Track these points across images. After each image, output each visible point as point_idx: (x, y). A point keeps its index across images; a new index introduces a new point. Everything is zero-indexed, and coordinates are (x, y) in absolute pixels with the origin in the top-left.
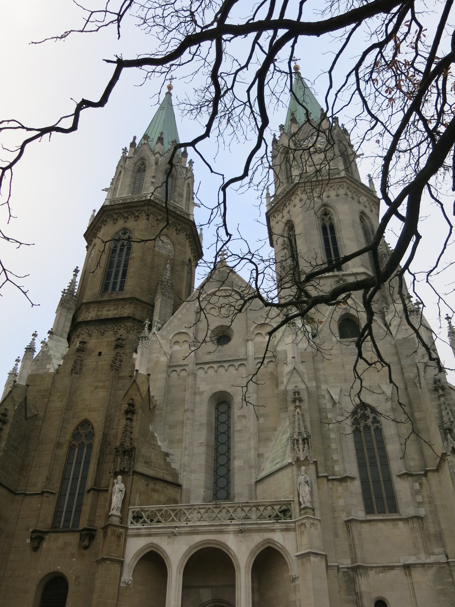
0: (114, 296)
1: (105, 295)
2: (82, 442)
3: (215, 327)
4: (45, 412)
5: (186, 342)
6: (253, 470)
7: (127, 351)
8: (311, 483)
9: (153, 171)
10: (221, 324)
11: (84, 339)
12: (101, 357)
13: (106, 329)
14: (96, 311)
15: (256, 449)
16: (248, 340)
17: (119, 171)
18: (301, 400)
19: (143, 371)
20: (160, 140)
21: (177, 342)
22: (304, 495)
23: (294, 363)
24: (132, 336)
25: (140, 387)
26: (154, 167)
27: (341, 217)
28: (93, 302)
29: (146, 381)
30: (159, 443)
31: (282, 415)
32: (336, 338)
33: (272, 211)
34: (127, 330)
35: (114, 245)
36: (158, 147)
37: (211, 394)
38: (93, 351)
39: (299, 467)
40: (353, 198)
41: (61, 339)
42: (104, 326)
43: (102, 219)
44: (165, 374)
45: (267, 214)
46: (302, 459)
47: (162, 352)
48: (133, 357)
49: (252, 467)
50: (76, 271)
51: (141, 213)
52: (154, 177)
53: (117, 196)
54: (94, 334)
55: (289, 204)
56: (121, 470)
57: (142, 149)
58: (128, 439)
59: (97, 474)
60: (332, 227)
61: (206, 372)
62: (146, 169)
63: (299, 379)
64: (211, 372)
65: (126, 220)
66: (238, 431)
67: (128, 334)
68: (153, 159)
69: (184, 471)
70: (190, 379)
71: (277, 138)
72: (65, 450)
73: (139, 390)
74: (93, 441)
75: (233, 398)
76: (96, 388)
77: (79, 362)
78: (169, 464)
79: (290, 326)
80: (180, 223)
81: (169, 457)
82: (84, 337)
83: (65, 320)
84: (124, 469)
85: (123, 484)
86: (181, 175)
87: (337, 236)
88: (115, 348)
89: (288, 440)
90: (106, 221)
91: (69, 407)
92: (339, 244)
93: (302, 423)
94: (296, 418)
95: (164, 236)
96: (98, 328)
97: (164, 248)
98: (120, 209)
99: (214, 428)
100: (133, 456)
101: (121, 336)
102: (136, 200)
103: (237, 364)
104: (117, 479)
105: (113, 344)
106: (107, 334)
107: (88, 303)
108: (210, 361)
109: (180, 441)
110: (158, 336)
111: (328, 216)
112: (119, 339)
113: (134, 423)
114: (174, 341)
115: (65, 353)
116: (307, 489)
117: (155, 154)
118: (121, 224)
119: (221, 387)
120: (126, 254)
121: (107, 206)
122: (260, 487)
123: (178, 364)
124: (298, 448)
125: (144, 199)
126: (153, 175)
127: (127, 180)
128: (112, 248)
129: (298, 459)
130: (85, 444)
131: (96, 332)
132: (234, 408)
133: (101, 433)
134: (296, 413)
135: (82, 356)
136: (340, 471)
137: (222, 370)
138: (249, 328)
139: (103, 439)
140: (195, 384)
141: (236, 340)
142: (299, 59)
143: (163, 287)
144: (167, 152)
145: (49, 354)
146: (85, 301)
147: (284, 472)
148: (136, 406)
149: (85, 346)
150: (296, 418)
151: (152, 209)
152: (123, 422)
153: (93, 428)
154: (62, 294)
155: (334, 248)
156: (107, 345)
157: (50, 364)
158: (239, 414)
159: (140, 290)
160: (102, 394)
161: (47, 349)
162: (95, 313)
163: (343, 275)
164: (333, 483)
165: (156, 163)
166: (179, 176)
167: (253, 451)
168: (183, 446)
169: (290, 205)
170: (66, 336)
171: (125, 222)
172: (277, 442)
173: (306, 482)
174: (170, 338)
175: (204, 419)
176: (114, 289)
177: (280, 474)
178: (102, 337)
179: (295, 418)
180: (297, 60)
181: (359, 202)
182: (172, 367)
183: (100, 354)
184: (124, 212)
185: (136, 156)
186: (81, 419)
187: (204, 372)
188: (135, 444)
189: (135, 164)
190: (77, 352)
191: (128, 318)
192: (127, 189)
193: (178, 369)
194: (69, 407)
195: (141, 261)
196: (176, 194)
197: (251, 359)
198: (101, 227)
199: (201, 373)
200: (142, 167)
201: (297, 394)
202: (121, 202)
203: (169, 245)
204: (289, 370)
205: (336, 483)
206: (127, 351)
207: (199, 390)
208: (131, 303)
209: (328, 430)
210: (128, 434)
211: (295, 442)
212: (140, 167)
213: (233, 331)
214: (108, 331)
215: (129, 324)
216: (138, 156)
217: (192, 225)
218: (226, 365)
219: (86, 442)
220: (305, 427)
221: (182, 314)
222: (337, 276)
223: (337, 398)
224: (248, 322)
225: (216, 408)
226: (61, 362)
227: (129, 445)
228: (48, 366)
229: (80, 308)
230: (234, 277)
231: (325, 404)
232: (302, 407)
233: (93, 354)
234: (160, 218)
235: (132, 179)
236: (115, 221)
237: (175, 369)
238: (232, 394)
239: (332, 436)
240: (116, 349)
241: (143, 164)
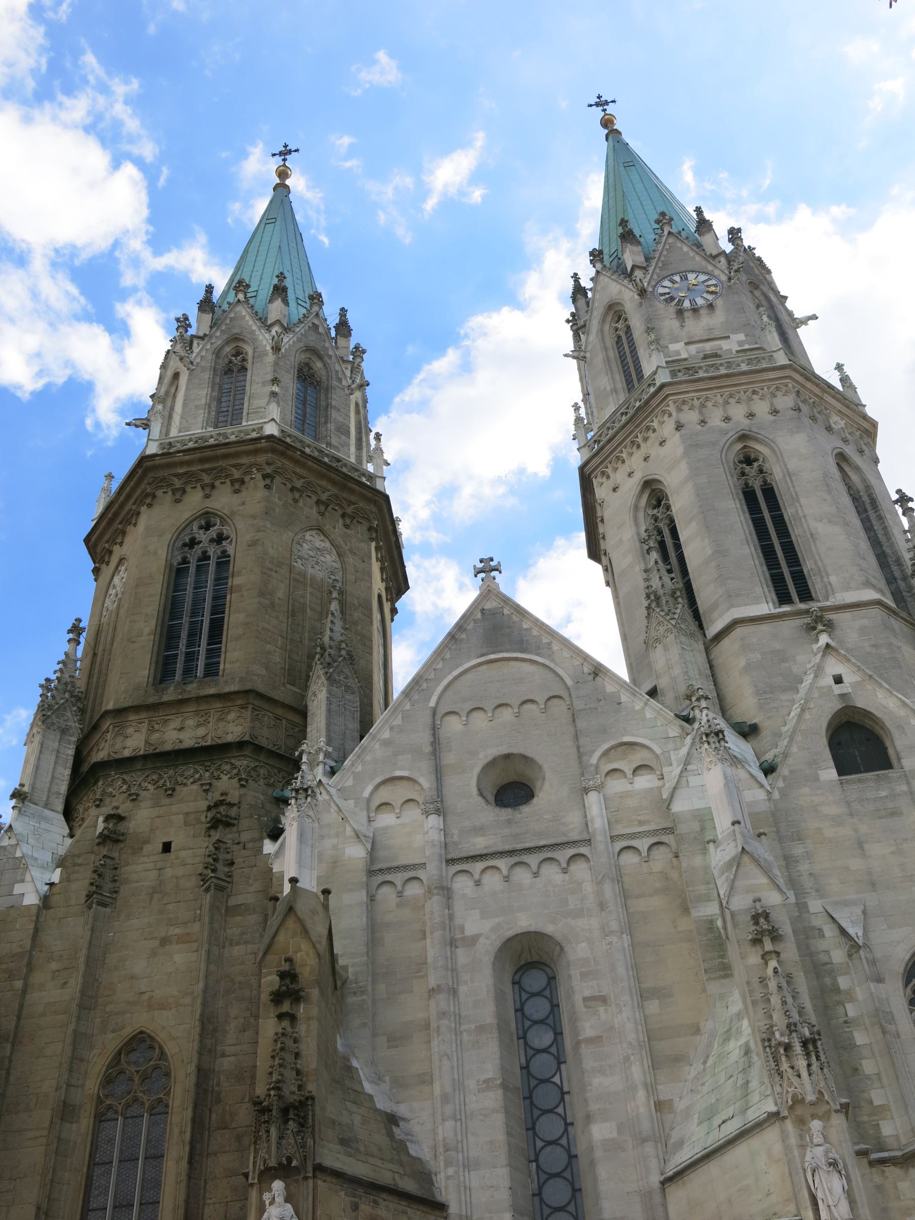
0: (192, 689)
1: (166, 689)
2: (136, 1100)
3: (490, 758)
4: (19, 1018)
5: (411, 804)
6: (649, 1148)
7: (245, 837)
8: (845, 1167)
9: (269, 369)
10: (506, 752)
11: (117, 808)
12: (172, 855)
13: (180, 779)
14: (144, 730)
15: (651, 1088)
16: (586, 790)
17: (170, 373)
18: (775, 936)
19: (310, 883)
20: (280, 291)
21: (385, 805)
22: (831, 1203)
23: (738, 836)
24: (255, 794)
25: (308, 923)
26: (271, 358)
27: (793, 464)
28: (137, 709)
29: (320, 909)
30: (368, 1088)
31: (714, 988)
32: (830, 773)
33: (597, 460)
34: (240, 780)
35: (179, 558)
36: (276, 310)
37: (498, 944)
38: (147, 842)
39: (801, 1122)
40: (813, 418)
41: (47, 813)
42: (171, 772)
43: (138, 492)
44: (364, 893)
45: (582, 469)
46: (811, 1097)
47: (349, 832)
48: (265, 852)
49: (644, 1140)
50: (76, 629)
51: (250, 473)
52: (275, 381)
53: (174, 432)
54: (143, 794)
55: (646, 439)
56: (280, 1164)
57: (232, 315)
58: (290, 1075)
59: (188, 1187)
60: (770, 492)
61: (478, 883)
62: (249, 366)
63: (764, 880)
64: (492, 881)
65: (207, 492)
66: (590, 1041)
67: (243, 791)
68: (265, 339)
69: (448, 1164)
70: (435, 904)
71: (586, 283)
72: (85, 1122)
73: (306, 932)
74: (168, 1094)
75: (562, 949)
76: (164, 941)
77: (108, 874)
78: (400, 1147)
79: (711, 740)
80: (353, 498)
81: (398, 1126)
82: (116, 804)
83: (56, 763)
84: (290, 1160)
85: (289, 1206)
86: (340, 380)
87: (788, 512)
88: (209, 828)
89: (747, 1052)
90: (154, 496)
91: (89, 1000)
92: (796, 533)
93: (790, 1000)
94: (772, 985)
95: (313, 533)
96: (155, 777)
97: (317, 563)
98: (188, 463)
99: (515, 1038)
100: (310, 1121)
101: (222, 795)
102: (233, 438)
103: (563, 855)
104: (270, 1190)
105: (203, 819)
106: (182, 791)
107: (119, 712)
108: (485, 852)
109: (426, 1079)
110: (333, 791)
111: (756, 464)
112: (217, 804)
113: (302, 1028)
114: (376, 802)
115: (62, 851)
116: (837, 1184)
117: (269, 328)
118: (194, 501)
119: (524, 923)
120: (216, 580)
121: (155, 455)
122: (678, 1195)
123: (396, 864)
124: (792, 1068)
125: (254, 435)
127: (196, 395)
128: (175, 564)
129: (798, 1101)
130: (143, 1104)
131: (150, 787)
132: (570, 977)
133: (192, 1068)
134: (770, 971)
135: (116, 855)
136: (897, 1137)
137: (522, 876)
138: (584, 758)
139: (198, 1085)
140: (451, 917)
141: (550, 793)
142: (613, 101)
143: (328, 659)
144: (300, 321)
145: (18, 854)
146: (110, 706)
147: (754, 1143)
148: (299, 982)
149: (121, 827)
150: (772, 985)
151: (279, 462)
152: (269, 1027)
153: (163, 1055)
154: (40, 691)
155: (782, 544)
156: (186, 823)
157: (23, 881)
158: (587, 993)
159: (264, 672)
160: (183, 958)
161: (13, 842)
162: (143, 739)
163: (822, 609)
164: (883, 1172)
165: (276, 349)
166: (335, 383)
167: (641, 1094)
168: (437, 1091)
169: (649, 442)
170: (60, 807)
171: (207, 496)
172: (710, 1062)
173: (830, 1164)
174: (366, 794)
175: (488, 1014)
176: (189, 671)
177: (740, 1152)
178: (167, 801)
179: (767, 986)
180: (607, 103)
181: (829, 429)
182: (378, 870)
183: (167, 847)
184: (202, 470)
185: (218, 334)
186: (128, 1031)
187: (471, 883)
188: (311, 1087)
189: (217, 353)
190: (98, 844)
191: (240, 745)
192: (201, 416)
193: (398, 878)
194: (89, 1000)
195: (262, 594)
196: (331, 426)
197: (600, 840)
198: (138, 514)
199: (462, 885)
201: (762, 920)
202: (191, 445)
203: (328, 556)
204: (728, 858)
205: (892, 1171)
206: (245, 837)
207: (463, 932)
208: (244, 707)
209: (846, 1022)
210: (290, 1058)
211: (776, 1051)
212: (231, 362)
213: (540, 767)
214: (185, 785)
215: (243, 763)
216: (222, 332)
217: (382, 502)
218: (533, 860)
219: (145, 1098)
220: (801, 1011)
221: (391, 728)
222: (807, 612)
223: (860, 934)
224: (582, 741)
225: (514, 983)
226: (56, 877)
227: (295, 1089)
228: (18, 889)
229: (95, 727)
230: (525, 626)
231: (827, 952)
232: (782, 956)
233: (148, 848)
234: (299, 484)
235: (213, 390)
236: (179, 495)
237: (388, 877)
238: (558, 937)
239: (860, 1038)
240: (212, 832)
241: (238, 353)
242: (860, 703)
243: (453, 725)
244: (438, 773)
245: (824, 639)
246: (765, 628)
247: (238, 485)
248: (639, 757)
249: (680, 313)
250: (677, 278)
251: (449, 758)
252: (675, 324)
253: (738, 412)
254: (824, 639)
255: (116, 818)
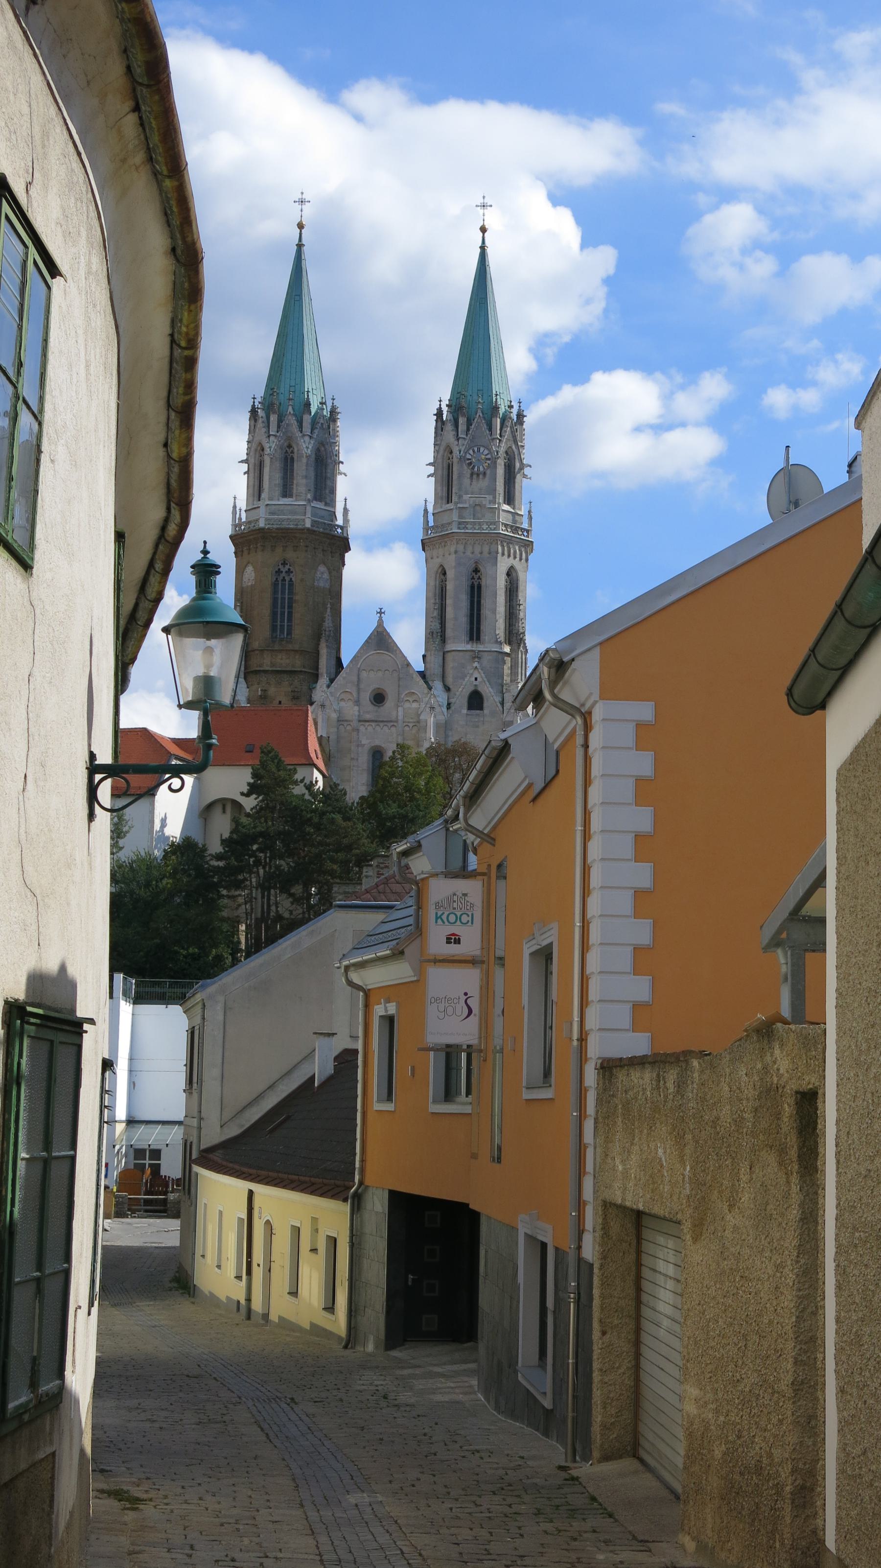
16: (398, 706)
32: (465, 711)
60: (479, 587)
64: (370, 728)
87: (482, 601)
103: (390, 724)
119: (377, 742)
126: (304, 474)
137: (378, 728)
141: (389, 703)
175: (365, 766)
193: (345, 724)
196: (327, 491)
197: (400, 722)
200: (289, 451)
218: (382, 724)
236: (273, 548)
241: (290, 446)
242: (479, 689)
243: (364, 674)
244: (359, 691)
245: (476, 664)
246: (461, 654)
247: (296, 548)
248: (415, 697)
249: (472, 475)
250: (476, 449)
251: (362, 686)
252: (468, 481)
253: (477, 549)
254: (476, 664)
255: (264, 691)
